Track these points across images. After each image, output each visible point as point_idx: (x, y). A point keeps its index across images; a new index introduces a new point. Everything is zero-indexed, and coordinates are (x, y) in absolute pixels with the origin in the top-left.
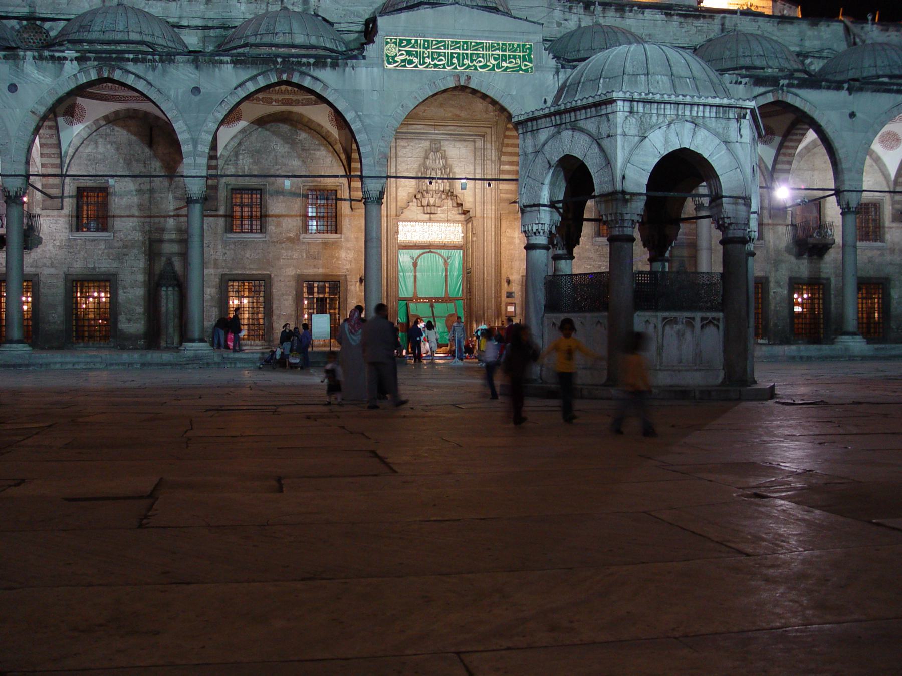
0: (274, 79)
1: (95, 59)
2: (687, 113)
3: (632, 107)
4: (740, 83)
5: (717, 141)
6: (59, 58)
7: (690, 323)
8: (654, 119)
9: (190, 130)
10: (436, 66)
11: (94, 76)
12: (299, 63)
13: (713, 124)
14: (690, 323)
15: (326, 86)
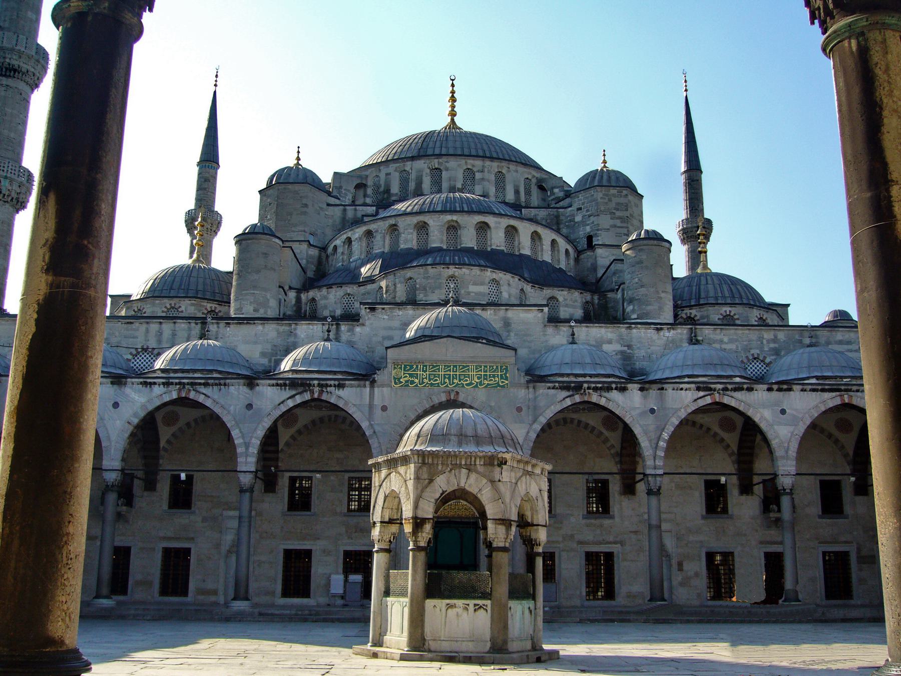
0: (307, 396)
1: (176, 384)
2: (463, 463)
3: (423, 460)
4: (682, 389)
5: (485, 481)
6: (151, 384)
7: (466, 609)
8: (440, 467)
9: (243, 437)
10: (432, 385)
11: (175, 395)
12: (327, 386)
13: (480, 469)
14: (466, 609)
15: (346, 403)
